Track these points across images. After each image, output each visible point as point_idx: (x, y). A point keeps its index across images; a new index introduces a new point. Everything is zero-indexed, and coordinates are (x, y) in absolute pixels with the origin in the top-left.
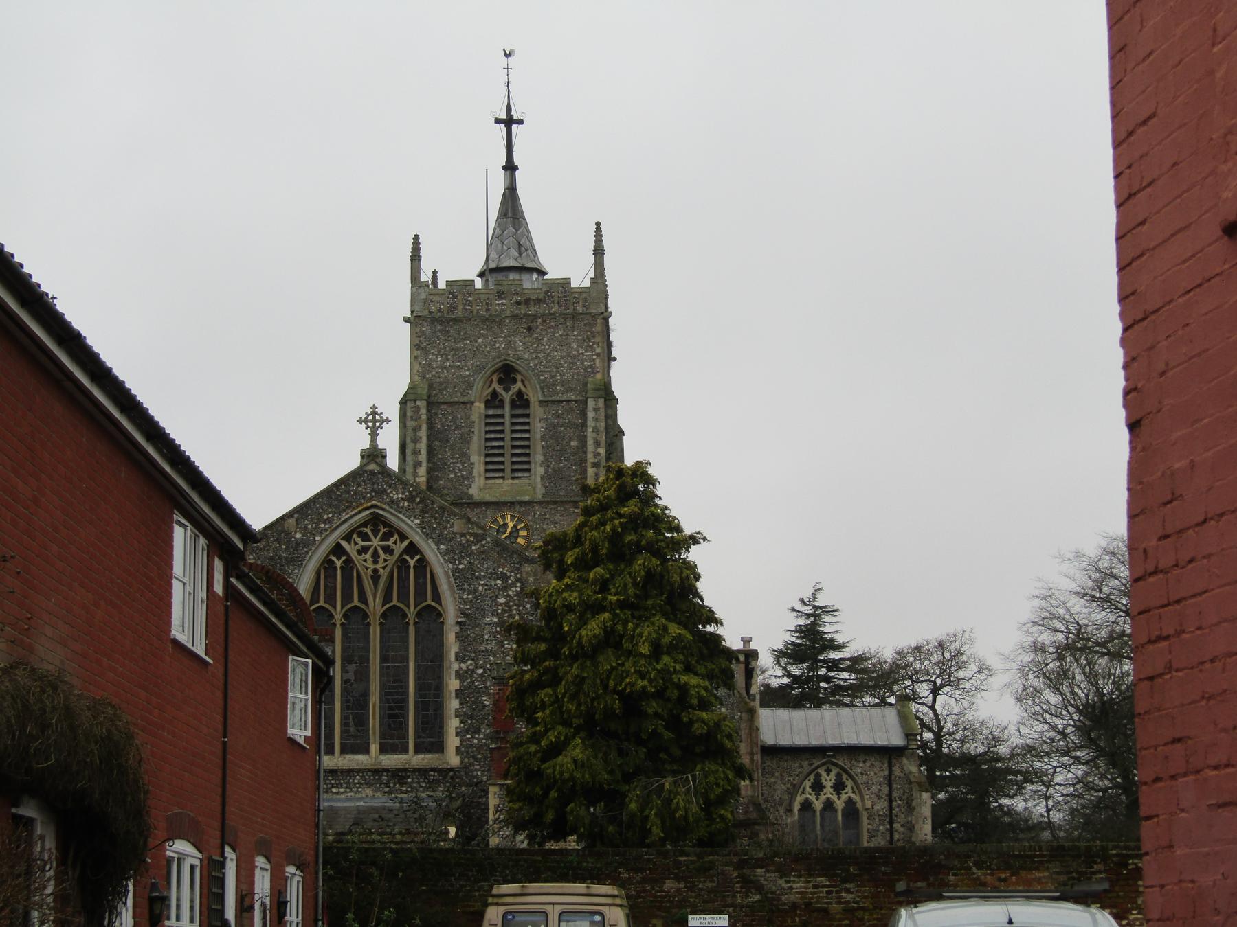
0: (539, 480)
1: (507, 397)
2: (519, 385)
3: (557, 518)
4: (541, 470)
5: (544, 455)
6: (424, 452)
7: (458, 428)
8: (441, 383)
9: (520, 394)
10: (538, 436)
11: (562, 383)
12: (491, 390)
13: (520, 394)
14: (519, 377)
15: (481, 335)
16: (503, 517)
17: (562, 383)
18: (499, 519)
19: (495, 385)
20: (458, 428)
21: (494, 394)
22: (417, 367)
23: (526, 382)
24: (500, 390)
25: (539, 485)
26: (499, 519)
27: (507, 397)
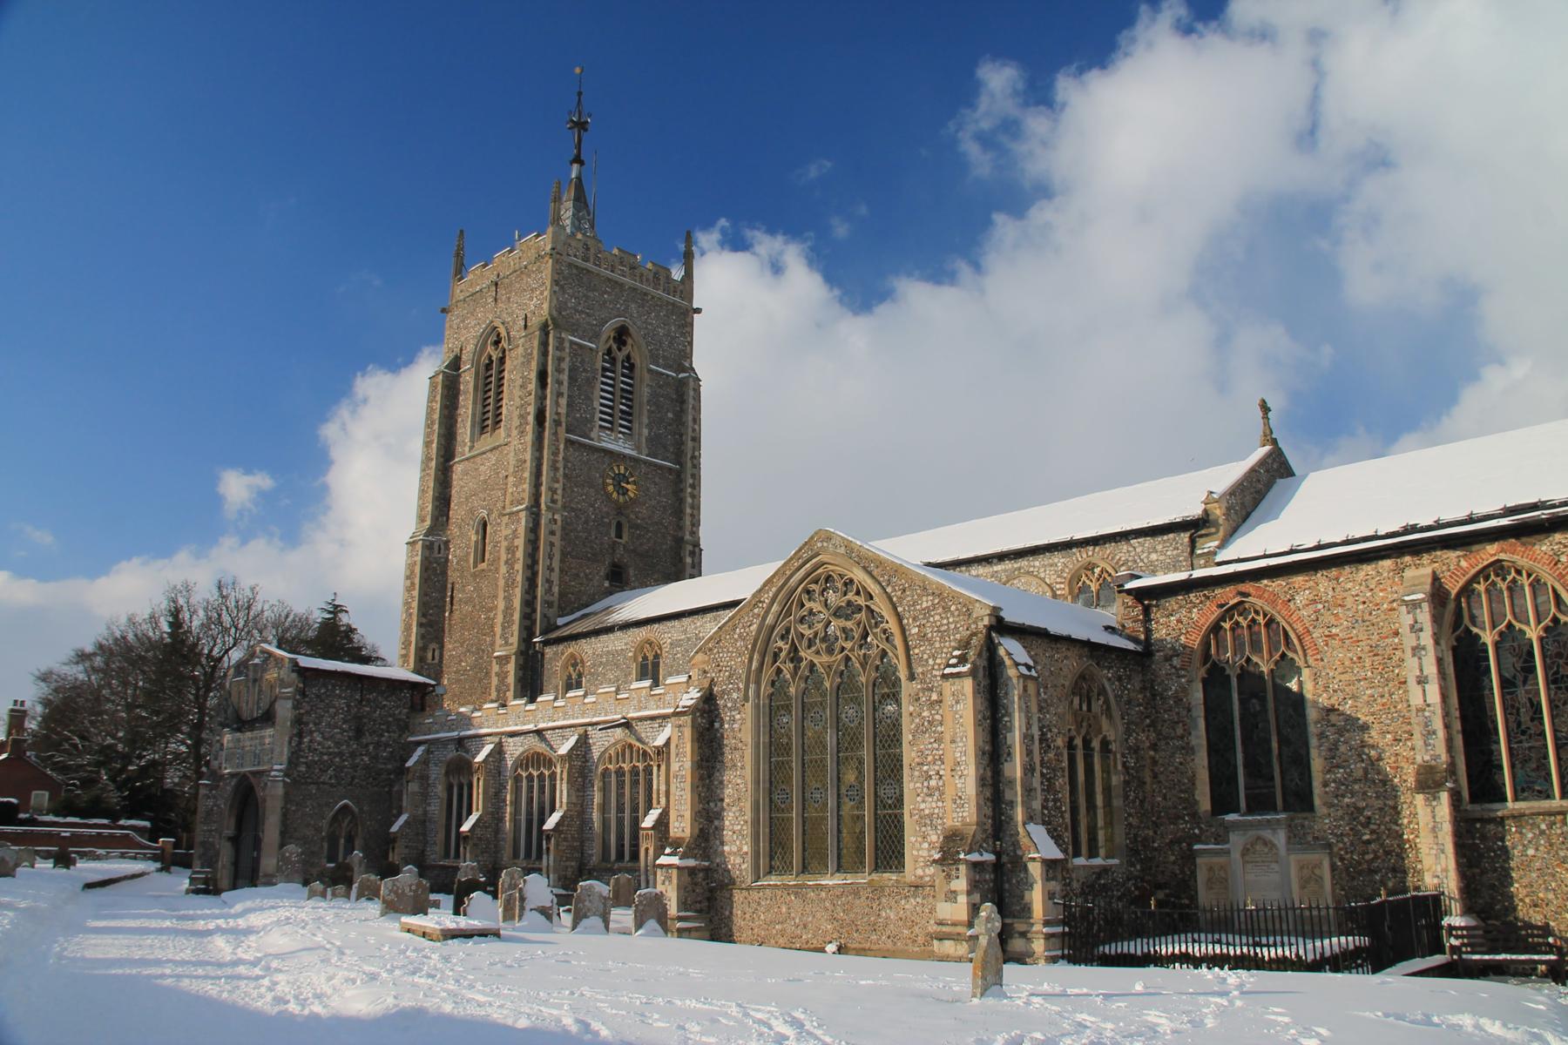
0: (644, 441)
1: (620, 356)
2: (626, 350)
3: (657, 480)
4: (645, 432)
5: (649, 418)
6: (566, 384)
7: (585, 370)
8: (574, 325)
9: (628, 357)
10: (645, 401)
11: (665, 358)
12: (608, 346)
13: (628, 357)
14: (630, 341)
15: (606, 292)
16: (618, 466)
17: (665, 358)
18: (615, 468)
19: (611, 341)
20: (585, 370)
21: (609, 352)
22: (555, 301)
23: (635, 347)
24: (615, 347)
25: (644, 445)
26: (615, 468)
27: (620, 356)
